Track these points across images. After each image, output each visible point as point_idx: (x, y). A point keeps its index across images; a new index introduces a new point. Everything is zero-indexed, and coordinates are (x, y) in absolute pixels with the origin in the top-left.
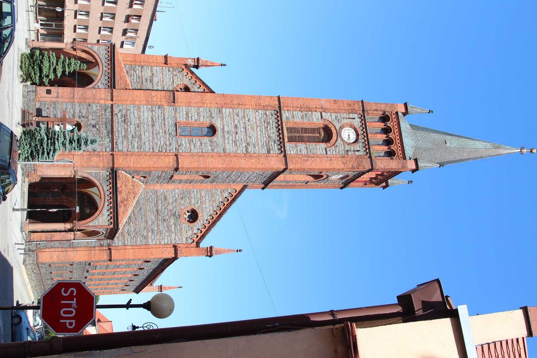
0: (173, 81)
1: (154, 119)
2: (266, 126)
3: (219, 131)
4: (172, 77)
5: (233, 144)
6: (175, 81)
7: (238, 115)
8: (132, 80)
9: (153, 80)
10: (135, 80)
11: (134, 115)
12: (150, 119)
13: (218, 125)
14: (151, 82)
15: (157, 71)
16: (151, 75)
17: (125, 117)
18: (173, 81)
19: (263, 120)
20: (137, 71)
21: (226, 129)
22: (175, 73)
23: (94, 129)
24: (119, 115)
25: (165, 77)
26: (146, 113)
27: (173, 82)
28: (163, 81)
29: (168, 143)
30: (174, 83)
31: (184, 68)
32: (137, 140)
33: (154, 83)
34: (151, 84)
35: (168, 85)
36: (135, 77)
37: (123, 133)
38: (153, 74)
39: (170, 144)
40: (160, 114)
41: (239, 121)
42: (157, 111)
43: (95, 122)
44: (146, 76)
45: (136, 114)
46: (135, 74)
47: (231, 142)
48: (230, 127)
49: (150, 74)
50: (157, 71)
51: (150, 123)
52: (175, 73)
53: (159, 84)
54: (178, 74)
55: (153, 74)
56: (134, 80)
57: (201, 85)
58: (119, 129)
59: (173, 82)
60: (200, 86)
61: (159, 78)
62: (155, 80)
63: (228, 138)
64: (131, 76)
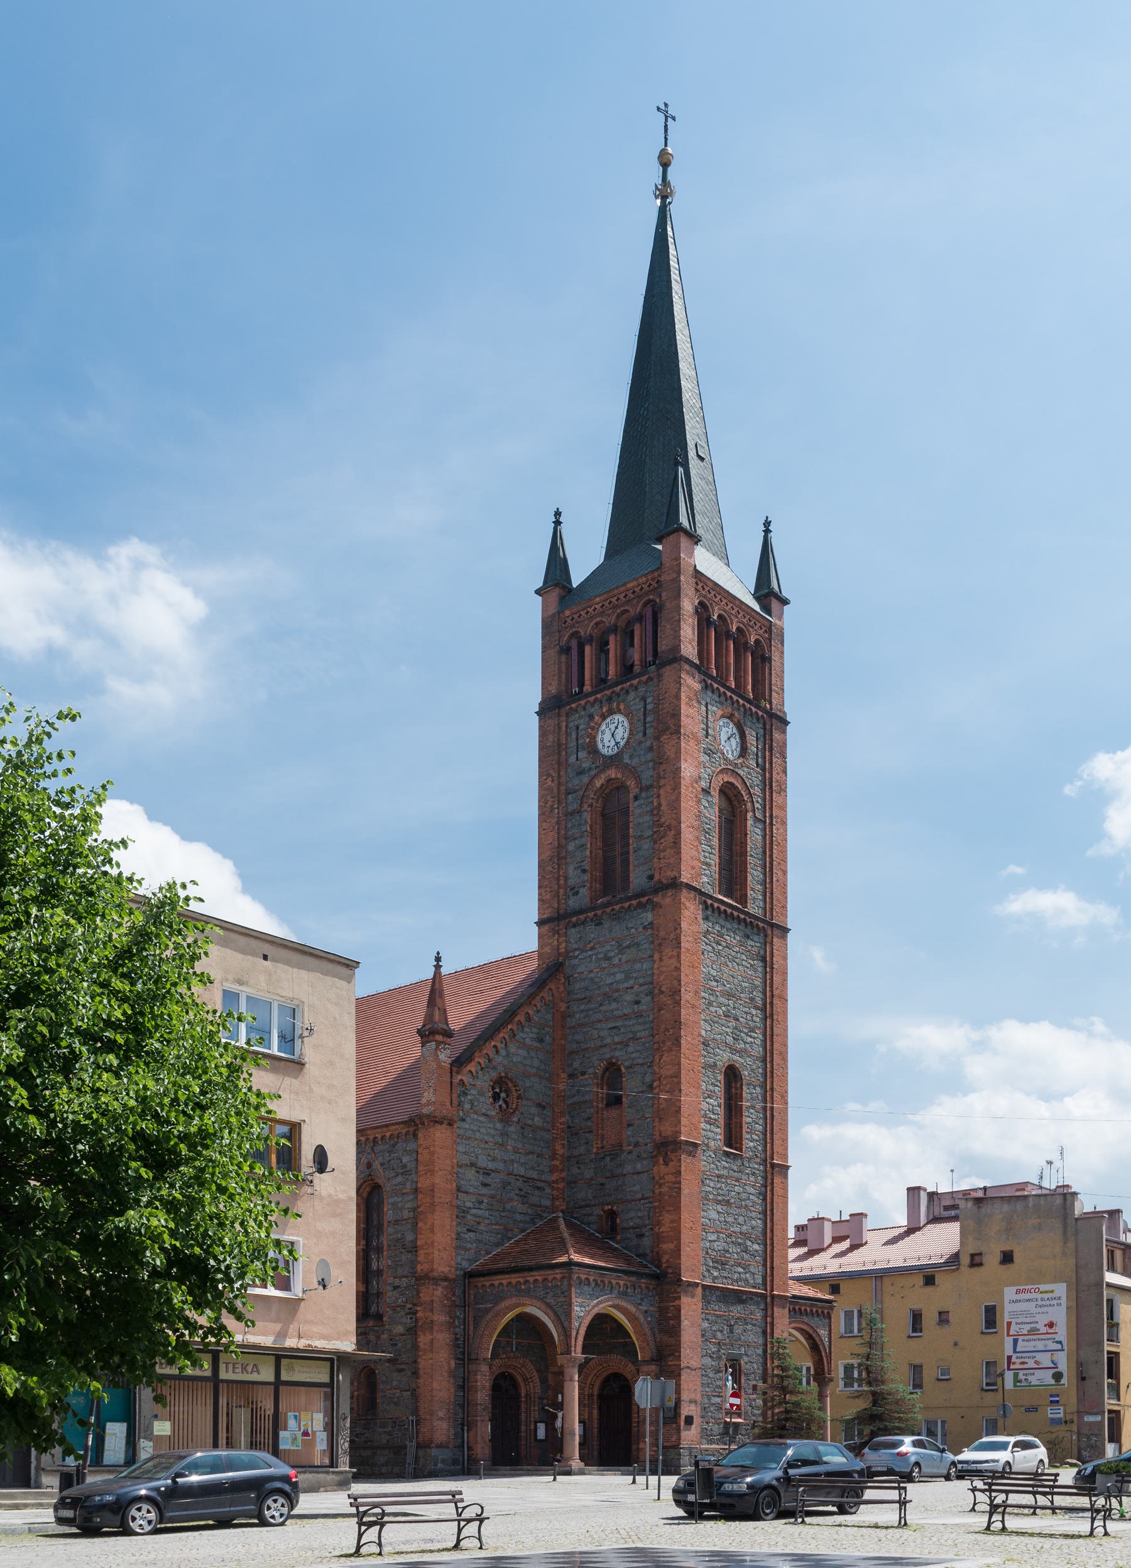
0: (484, 1115)
1: (720, 1198)
2: (724, 944)
3: (735, 1058)
4: (475, 1116)
5: (753, 1034)
6: (484, 1111)
7: (710, 1004)
8: (486, 1221)
9: (485, 1169)
10: (487, 1214)
11: (715, 1241)
12: (719, 1208)
13: (724, 1057)
14: (488, 1174)
15: (465, 1153)
16: (473, 1170)
17: (717, 1262)
18: (484, 1115)
19: (714, 945)
20: (468, 1204)
21: (730, 1040)
22: (467, 1106)
23: (738, 1330)
24: (716, 1274)
25: (478, 1135)
26: (713, 1215)
27: (486, 1115)
28: (486, 1142)
29: (752, 1179)
30: (489, 1113)
31: (459, 1077)
32: (749, 1243)
33: (491, 1166)
34: (493, 1174)
35: (493, 1132)
36: (479, 1212)
37: (741, 1270)
38: (472, 1165)
39: (753, 1174)
40: (712, 1184)
41: (720, 1005)
42: (708, 1189)
43: (725, 1327)
44: (476, 1183)
45: (713, 1237)
46: (474, 1211)
47: (749, 1039)
48: (728, 1030)
49: (471, 1174)
50: (465, 1153)
51: (724, 1208)
52: (467, 1106)
53: (491, 1153)
54: (469, 1097)
55: (472, 1165)
56: (487, 1215)
57: (493, 1043)
58: (736, 1276)
59: (486, 1115)
60: (495, 1046)
61: (480, 1151)
62: (483, 1162)
63: (745, 1043)
64: (479, 1223)
